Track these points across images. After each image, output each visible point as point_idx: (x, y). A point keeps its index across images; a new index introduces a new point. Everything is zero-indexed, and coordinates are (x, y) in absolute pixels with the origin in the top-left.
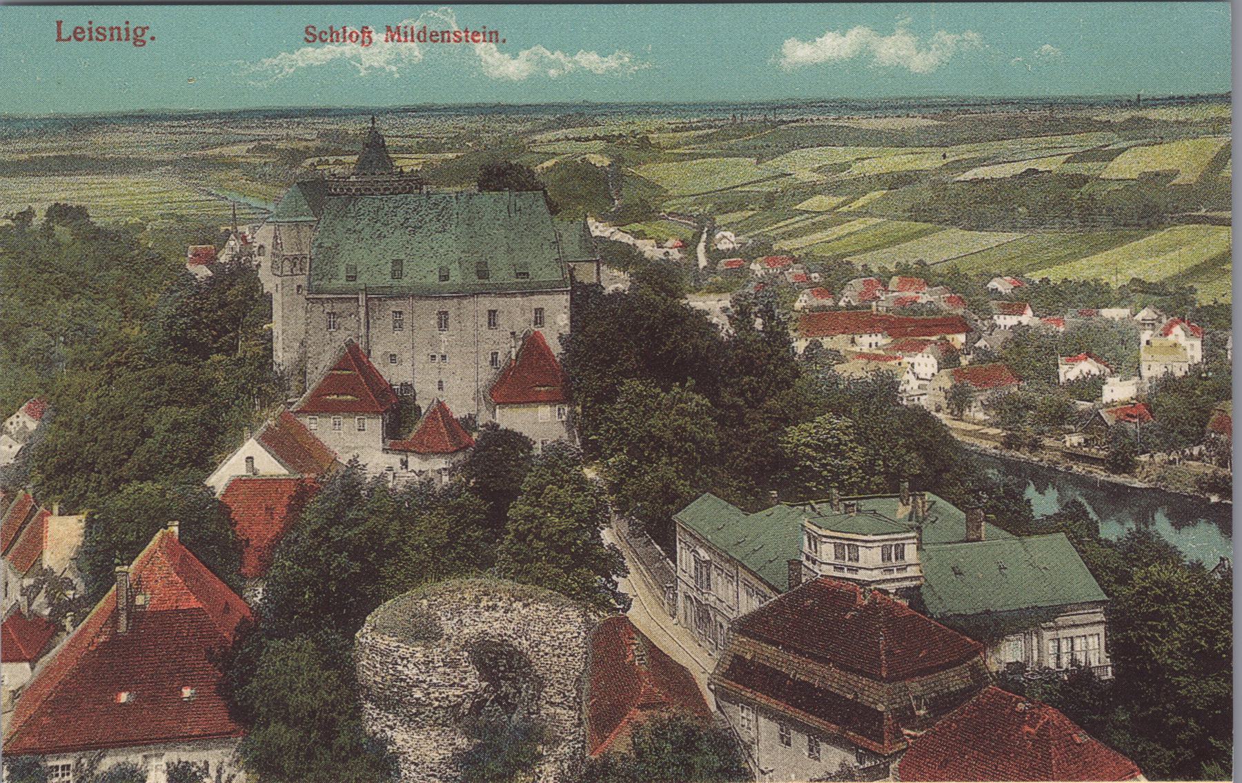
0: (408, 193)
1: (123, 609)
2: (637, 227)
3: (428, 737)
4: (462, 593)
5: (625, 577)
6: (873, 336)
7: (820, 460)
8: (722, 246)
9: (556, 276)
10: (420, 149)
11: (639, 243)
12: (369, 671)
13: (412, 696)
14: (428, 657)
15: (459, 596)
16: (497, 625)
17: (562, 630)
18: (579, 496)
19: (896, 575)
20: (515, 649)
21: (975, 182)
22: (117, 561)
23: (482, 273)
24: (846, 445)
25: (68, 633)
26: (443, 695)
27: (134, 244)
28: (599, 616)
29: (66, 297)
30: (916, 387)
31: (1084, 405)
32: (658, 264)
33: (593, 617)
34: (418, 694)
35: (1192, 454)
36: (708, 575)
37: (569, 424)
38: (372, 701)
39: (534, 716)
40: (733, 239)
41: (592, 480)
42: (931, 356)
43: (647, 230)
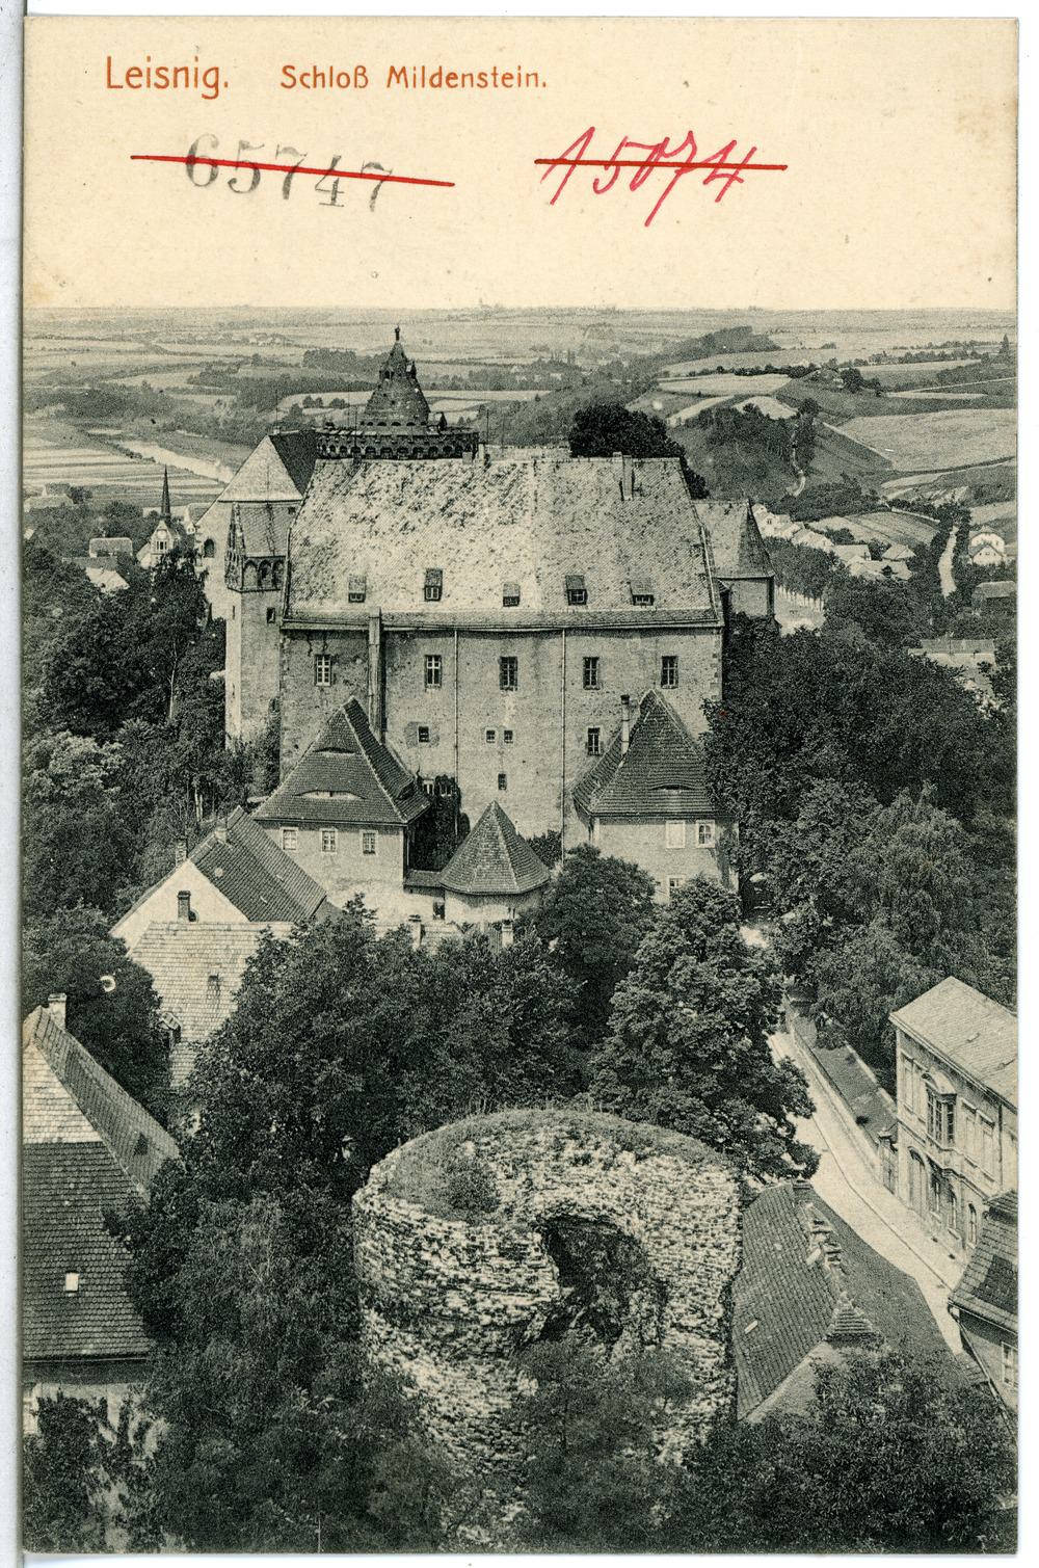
2: (837, 523)
5: (807, 1117)
8: (983, 559)
11: (841, 551)
13: (445, 1304)
15: (529, 1138)
16: (590, 1190)
17: (701, 1202)
23: (577, 596)
28: (764, 1182)
32: (872, 587)
34: (455, 1300)
38: (378, 1310)
41: (756, 949)
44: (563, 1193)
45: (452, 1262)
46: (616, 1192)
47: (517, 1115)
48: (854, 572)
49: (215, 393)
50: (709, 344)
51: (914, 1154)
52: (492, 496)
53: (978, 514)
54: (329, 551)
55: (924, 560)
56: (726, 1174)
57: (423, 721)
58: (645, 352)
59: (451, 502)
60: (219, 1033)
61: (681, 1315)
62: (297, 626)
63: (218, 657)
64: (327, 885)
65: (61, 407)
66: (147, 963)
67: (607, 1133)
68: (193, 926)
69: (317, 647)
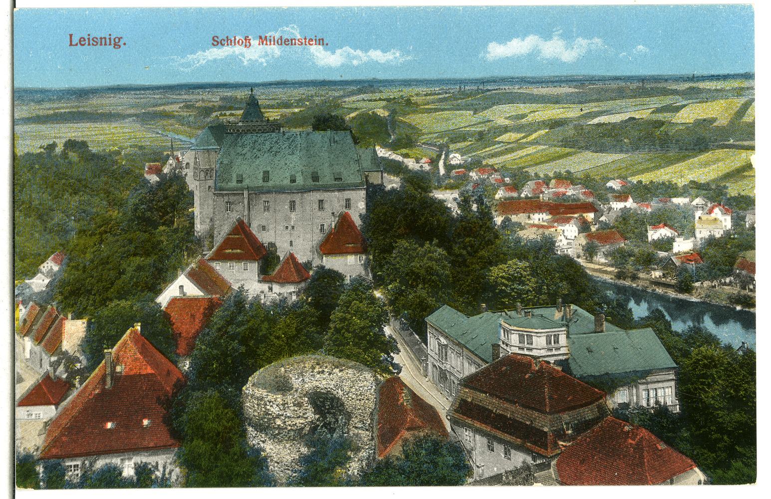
0: (272, 132)
1: (108, 374)
2: (404, 151)
3: (285, 447)
4: (304, 364)
5: (398, 354)
7: (510, 286)
8: (453, 162)
10: (279, 106)
11: (406, 160)
12: (251, 408)
13: (275, 424)
15: (302, 365)
16: (324, 382)
17: (362, 385)
19: (554, 352)
20: (335, 396)
21: (599, 125)
22: (105, 346)
23: (315, 178)
24: (525, 277)
25: (77, 388)
26: (293, 423)
28: (383, 377)
29: (75, 193)
30: (565, 244)
31: (662, 254)
32: (416, 172)
33: (379, 377)
34: (278, 422)
35: (725, 282)
36: (446, 353)
37: (366, 266)
38: (252, 427)
39: (346, 435)
41: (379, 298)
43: (410, 152)
44: (315, 383)
45: (277, 409)
51: (434, 366)
57: (264, 223)
67: (329, 362)
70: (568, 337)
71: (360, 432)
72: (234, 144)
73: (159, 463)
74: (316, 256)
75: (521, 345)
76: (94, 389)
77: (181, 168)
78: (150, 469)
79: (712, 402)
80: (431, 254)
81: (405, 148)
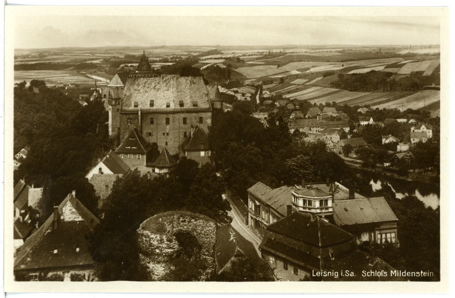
1: (56, 221)
2: (235, 89)
4: (173, 216)
5: (230, 211)
6: (317, 128)
7: (299, 170)
8: (265, 96)
9: (207, 106)
11: (236, 95)
14: (161, 238)
15: (172, 217)
16: (185, 227)
17: (208, 229)
18: (214, 182)
19: (324, 211)
21: (353, 74)
22: (54, 204)
23: (182, 104)
24: (307, 165)
25: (37, 229)
27: (62, 94)
29: (38, 112)
30: (332, 145)
31: (391, 152)
32: (243, 102)
33: (219, 225)
34: (157, 251)
35: (428, 169)
36: (259, 210)
39: (198, 259)
40: (269, 94)
42: (337, 135)
43: (239, 91)
45: (157, 243)
46: (191, 227)
47: (171, 212)
48: (239, 99)
49: (106, 64)
50: (209, 53)
52: (164, 85)
53: (264, 87)
54: (130, 97)
55: (253, 96)
56: (213, 224)
57: (150, 131)
58: (195, 54)
59: (155, 86)
60: (108, 197)
61: (204, 252)
62: (123, 112)
63: (107, 120)
64: (130, 166)
65: (73, 68)
66: (92, 183)
67: (189, 215)
68: (102, 175)
69: (128, 116)
70: (333, 202)
71: (207, 257)
72: (133, 84)
73: (86, 274)
74: (181, 151)
75: (305, 206)
76: (47, 230)
77: (101, 98)
78: (80, 278)
79: (420, 242)
80: (251, 151)
81: (236, 87)
